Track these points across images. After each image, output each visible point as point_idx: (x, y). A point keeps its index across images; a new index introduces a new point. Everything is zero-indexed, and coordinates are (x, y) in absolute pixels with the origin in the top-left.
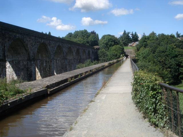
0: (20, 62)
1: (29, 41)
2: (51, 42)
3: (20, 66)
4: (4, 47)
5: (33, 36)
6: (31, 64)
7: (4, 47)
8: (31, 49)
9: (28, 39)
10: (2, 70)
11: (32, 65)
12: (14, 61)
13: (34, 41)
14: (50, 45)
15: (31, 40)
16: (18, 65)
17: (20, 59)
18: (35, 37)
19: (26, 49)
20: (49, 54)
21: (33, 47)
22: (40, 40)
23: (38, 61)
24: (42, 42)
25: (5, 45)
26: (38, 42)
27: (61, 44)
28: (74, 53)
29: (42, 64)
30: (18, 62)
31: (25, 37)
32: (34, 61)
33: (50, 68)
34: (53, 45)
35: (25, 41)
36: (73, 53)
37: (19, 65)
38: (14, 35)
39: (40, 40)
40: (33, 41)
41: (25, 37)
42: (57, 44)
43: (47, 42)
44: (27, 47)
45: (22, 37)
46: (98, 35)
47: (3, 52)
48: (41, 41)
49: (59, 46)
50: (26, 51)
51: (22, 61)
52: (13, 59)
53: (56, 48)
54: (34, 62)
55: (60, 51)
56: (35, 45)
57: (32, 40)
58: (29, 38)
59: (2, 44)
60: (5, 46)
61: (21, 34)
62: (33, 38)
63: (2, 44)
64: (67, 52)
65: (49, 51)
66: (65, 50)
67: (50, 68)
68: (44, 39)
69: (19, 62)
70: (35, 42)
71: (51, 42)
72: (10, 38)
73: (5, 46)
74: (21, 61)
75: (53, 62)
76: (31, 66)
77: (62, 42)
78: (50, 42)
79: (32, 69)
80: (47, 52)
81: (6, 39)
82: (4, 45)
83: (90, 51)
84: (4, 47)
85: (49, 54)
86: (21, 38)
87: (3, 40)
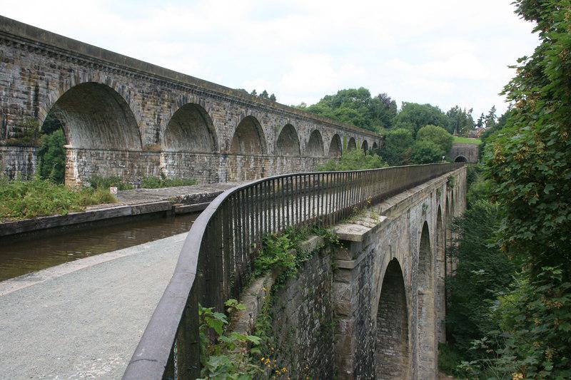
1: (218, 111)
5: (225, 100)
14: (266, 122)
19: (208, 129)
24: (249, 114)
32: (225, 155)
34: (274, 123)
42: (285, 122)
43: (260, 116)
44: (212, 124)
45: (200, 101)
47: (155, 132)
48: (246, 112)
56: (230, 120)
57: (224, 109)
61: (199, 94)
62: (228, 104)
63: (155, 114)
65: (264, 137)
68: (252, 107)
69: (193, 155)
71: (269, 115)
72: (173, 102)
80: (260, 137)
81: (163, 103)
84: (159, 119)
86: (198, 103)
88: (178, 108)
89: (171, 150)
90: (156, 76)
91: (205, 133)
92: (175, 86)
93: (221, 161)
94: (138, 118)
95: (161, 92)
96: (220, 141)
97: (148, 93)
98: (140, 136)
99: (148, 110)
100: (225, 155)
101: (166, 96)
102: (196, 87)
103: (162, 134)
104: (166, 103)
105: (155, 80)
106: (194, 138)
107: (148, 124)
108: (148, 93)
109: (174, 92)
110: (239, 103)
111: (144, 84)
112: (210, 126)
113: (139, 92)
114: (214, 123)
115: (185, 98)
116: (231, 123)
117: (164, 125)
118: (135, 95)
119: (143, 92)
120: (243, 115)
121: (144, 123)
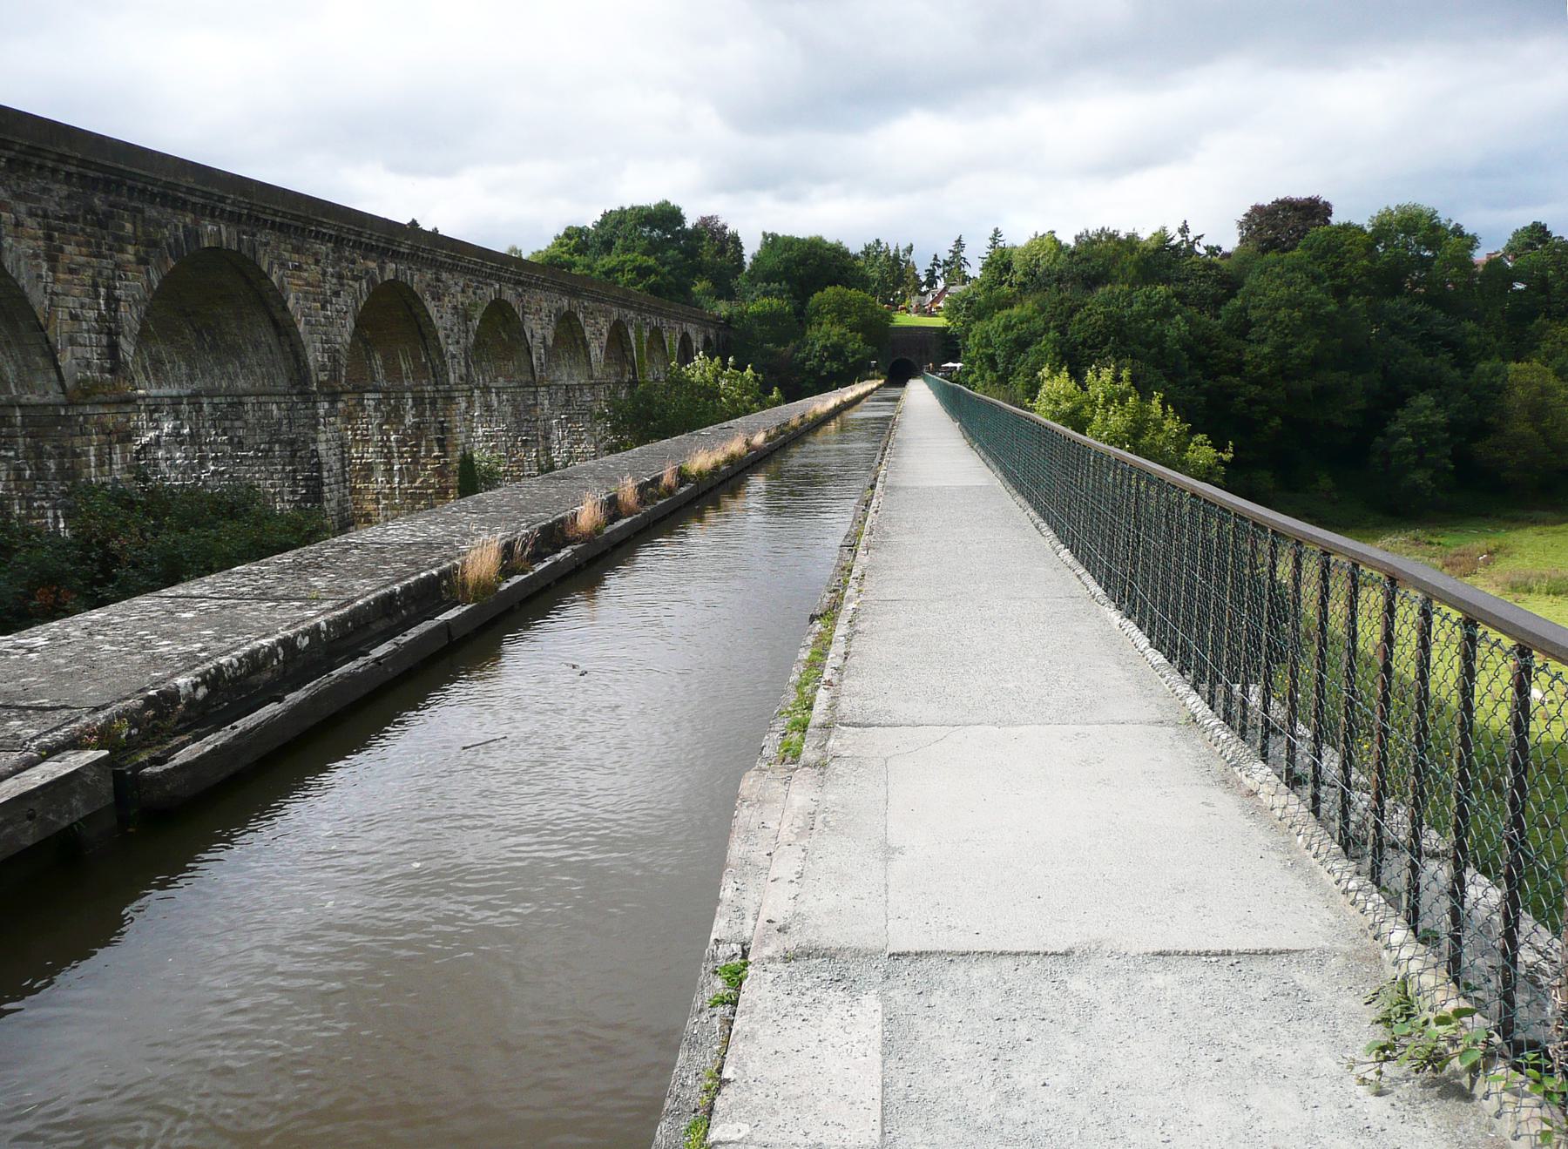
0: (241, 404)
1: (298, 268)
2: (444, 276)
3: (241, 432)
4: (112, 301)
5: (318, 235)
6: (315, 416)
7: (107, 304)
8: (308, 323)
9: (287, 255)
10: (99, 456)
11: (318, 423)
12: (205, 401)
13: (330, 270)
14: (437, 297)
15: (311, 261)
16: (227, 423)
17: (241, 384)
18: (339, 242)
20: (434, 355)
21: (323, 308)
22: (372, 265)
23: (367, 395)
24: (389, 275)
25: (118, 292)
26: (356, 278)
27: (509, 295)
28: (596, 351)
29: (394, 416)
30: (230, 405)
31: (267, 244)
32: (333, 397)
35: (265, 269)
36: (586, 346)
37: (238, 424)
38: (185, 226)
39: (372, 265)
40: (324, 274)
41: (267, 244)
42: (490, 293)
43: (419, 280)
44: (285, 309)
45: (240, 241)
46: (735, 240)
47: (104, 340)
48: (382, 269)
49: (499, 308)
50: (279, 335)
51: (253, 399)
52: (197, 385)
53: (478, 315)
54: (333, 403)
55: (504, 336)
58: (296, 250)
59: (95, 285)
60: (118, 300)
61: (234, 219)
62: (324, 249)
63: (95, 285)
64: (550, 342)
65: (437, 338)
66: (538, 328)
68: (396, 256)
70: (340, 277)
71: (444, 276)
72: (153, 244)
73: (118, 300)
74: (245, 399)
75: (464, 405)
76: (315, 427)
77: (519, 283)
78: (438, 280)
79: (322, 447)
80: (424, 338)
81: (122, 251)
82: (110, 289)
83: (693, 335)
84: (112, 301)
85: (434, 355)
86: (234, 247)
87: (99, 255)
88: (172, 263)
89: (166, 391)
90: (83, 163)
91: (267, 337)
92: (153, 195)
93: (321, 412)
94: (38, 300)
95: (109, 216)
96: (315, 356)
97: (66, 219)
98: (51, 355)
99: (71, 271)
100: (333, 397)
101: (129, 226)
102: (222, 199)
103: (127, 348)
104: (130, 249)
105: (82, 177)
106: (235, 352)
107: (74, 317)
108: (66, 219)
109: (151, 212)
110: (357, 245)
111: (45, 190)
112: (278, 316)
113: (31, 214)
114: (290, 304)
115: (193, 235)
116: (344, 301)
117: (130, 316)
118: (18, 224)
119: (45, 216)
120: (372, 281)
121: (62, 314)
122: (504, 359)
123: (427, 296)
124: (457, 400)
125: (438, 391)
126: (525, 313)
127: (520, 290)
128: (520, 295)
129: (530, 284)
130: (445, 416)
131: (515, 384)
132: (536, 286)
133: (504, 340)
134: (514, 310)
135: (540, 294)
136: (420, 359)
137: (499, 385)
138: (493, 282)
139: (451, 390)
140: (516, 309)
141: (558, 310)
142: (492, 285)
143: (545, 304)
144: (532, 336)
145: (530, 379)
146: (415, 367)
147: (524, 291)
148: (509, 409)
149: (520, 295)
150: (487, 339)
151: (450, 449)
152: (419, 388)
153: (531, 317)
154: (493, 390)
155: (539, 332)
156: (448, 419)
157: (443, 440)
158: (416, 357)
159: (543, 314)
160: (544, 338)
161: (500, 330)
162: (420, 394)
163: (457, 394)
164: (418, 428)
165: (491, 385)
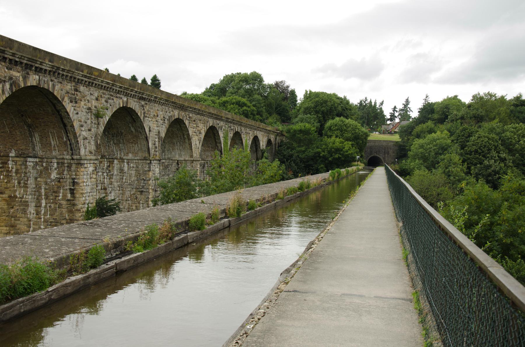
20: (71, 137)
33: (72, 191)
55: (133, 130)
67: (72, 191)
122: (132, 143)
123: (66, 99)
124: (86, 166)
125: (73, 159)
126: (145, 117)
127: (143, 103)
128: (143, 106)
129: (150, 101)
130: (76, 175)
131: (138, 158)
132: (155, 102)
133: (132, 131)
134: (137, 114)
135: (157, 107)
136: (63, 139)
137: (128, 158)
138: (122, 96)
139: (81, 159)
140: (139, 114)
141: (170, 117)
142: (121, 98)
143: (161, 113)
144: (150, 131)
145: (147, 155)
146: (60, 143)
147: (146, 104)
148: (133, 172)
149: (143, 106)
150: (123, 131)
151: (77, 196)
152: (61, 157)
153: (150, 119)
154: (125, 161)
155: (155, 129)
156: (78, 177)
157: (73, 190)
158: (60, 137)
159: (159, 119)
160: (159, 132)
161: (130, 125)
162: (61, 161)
163: (86, 162)
164: (59, 182)
165: (124, 158)
